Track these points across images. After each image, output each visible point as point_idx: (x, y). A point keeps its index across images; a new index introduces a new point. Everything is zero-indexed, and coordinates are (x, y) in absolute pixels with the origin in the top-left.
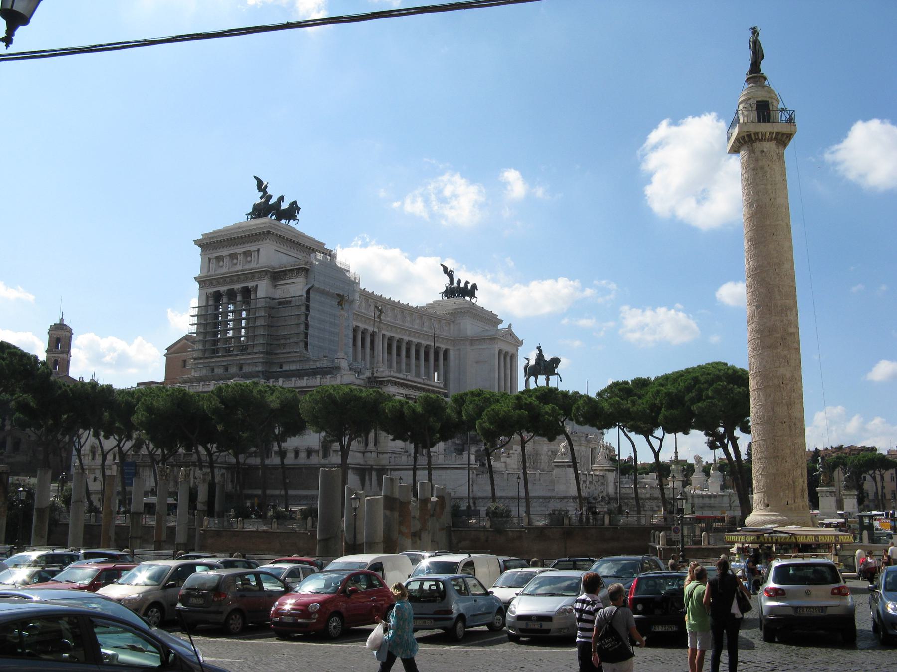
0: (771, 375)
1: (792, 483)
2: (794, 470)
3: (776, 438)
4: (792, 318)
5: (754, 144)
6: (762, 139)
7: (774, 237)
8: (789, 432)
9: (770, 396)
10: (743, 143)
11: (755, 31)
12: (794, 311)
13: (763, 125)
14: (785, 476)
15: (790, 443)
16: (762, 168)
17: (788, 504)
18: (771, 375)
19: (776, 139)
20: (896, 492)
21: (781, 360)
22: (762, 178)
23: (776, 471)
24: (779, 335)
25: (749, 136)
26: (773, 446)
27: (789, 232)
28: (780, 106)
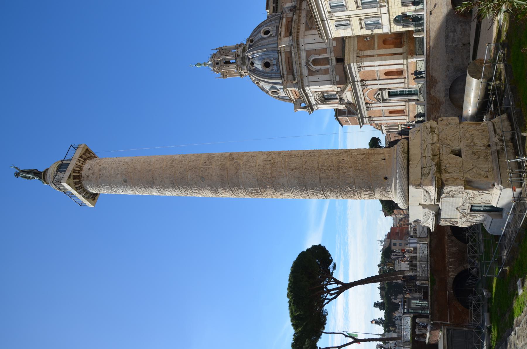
0: (262, 170)
1: (364, 156)
2: (352, 154)
5: (83, 176)
6: (80, 168)
7: (152, 164)
8: (316, 157)
9: (280, 172)
10: (79, 185)
14: (356, 161)
15: (326, 157)
17: (385, 159)
18: (262, 170)
21: (250, 161)
22: (107, 171)
23: (351, 169)
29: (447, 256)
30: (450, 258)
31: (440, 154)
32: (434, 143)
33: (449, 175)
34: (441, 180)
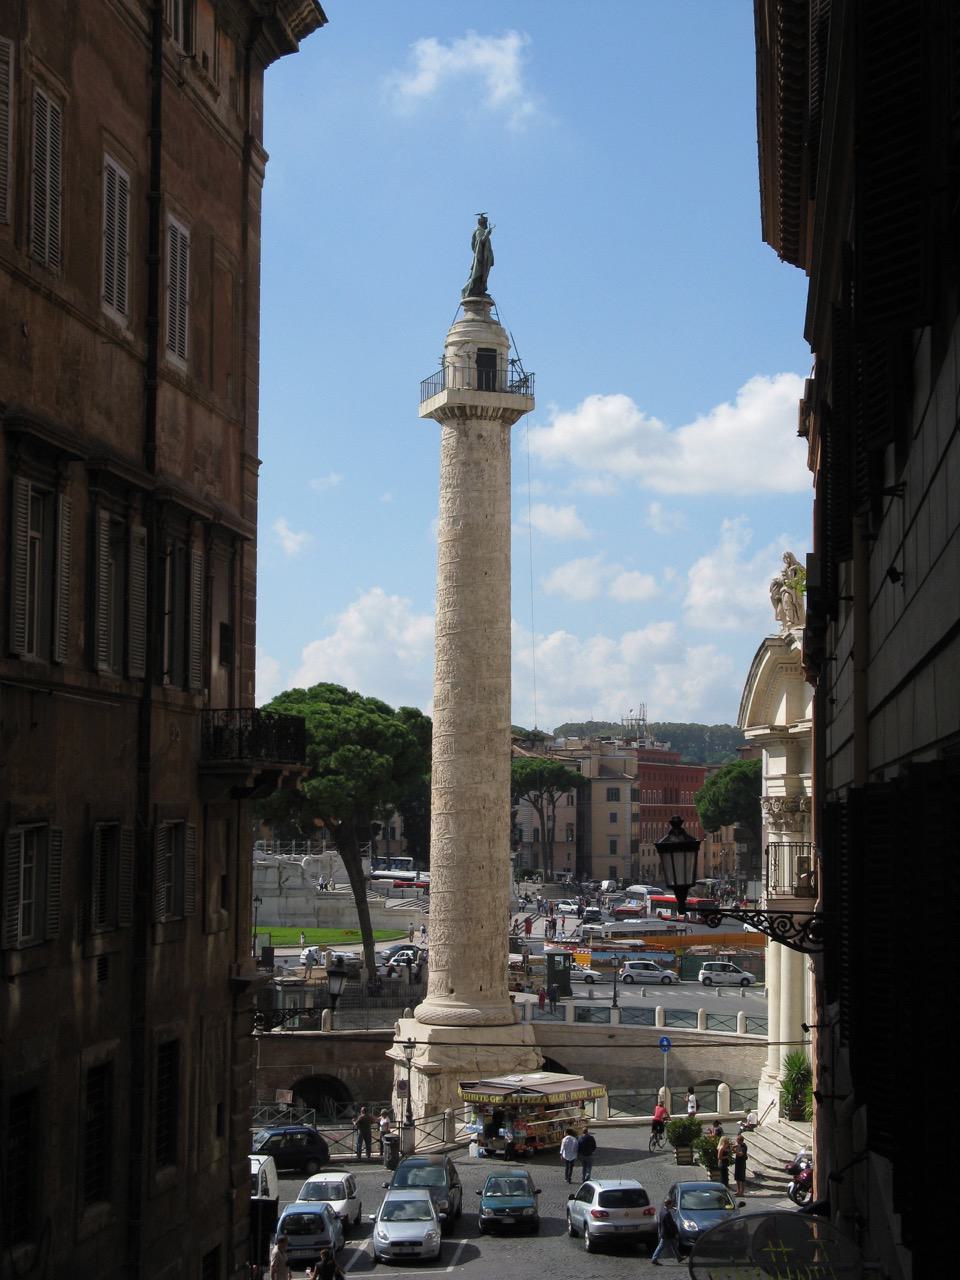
3: (470, 890)
4: (503, 706)
5: (468, 422)
11: (483, 222)
12: (507, 696)
13: (485, 394)
16: (477, 464)
18: (467, 795)
19: (502, 417)
20: (575, 828)
21: (484, 772)
24: (483, 733)
25: (462, 408)
26: (464, 902)
27: (508, 568)
28: (511, 355)
29: (379, 1064)
30: (374, 1070)
31: (481, 1072)
32: (498, 1064)
33: (446, 1083)
34: (439, 1074)
